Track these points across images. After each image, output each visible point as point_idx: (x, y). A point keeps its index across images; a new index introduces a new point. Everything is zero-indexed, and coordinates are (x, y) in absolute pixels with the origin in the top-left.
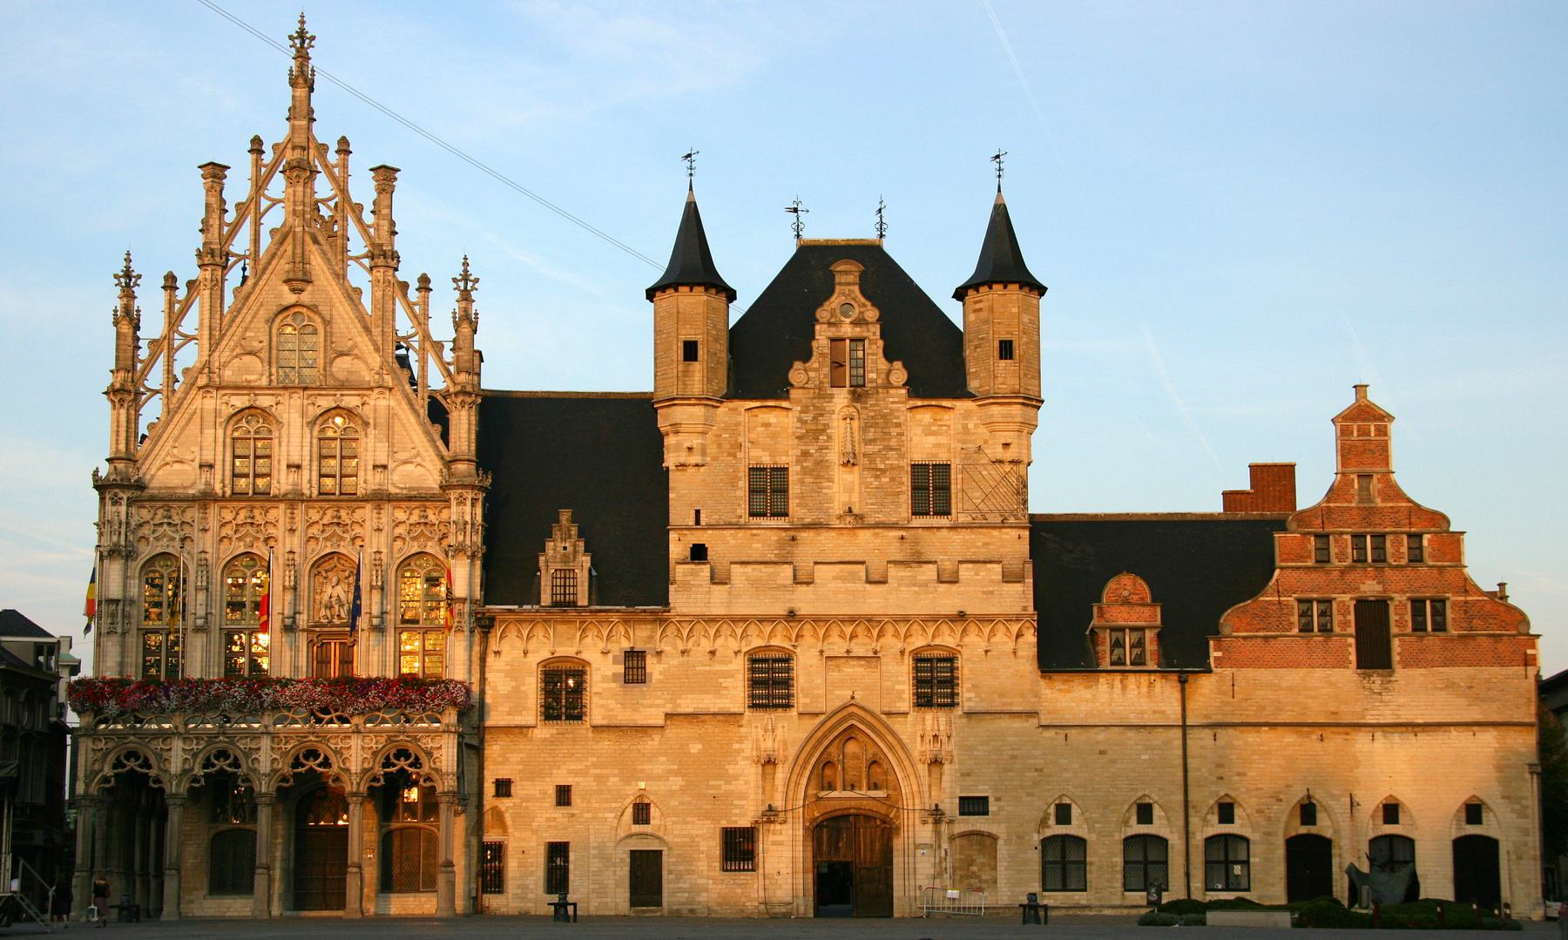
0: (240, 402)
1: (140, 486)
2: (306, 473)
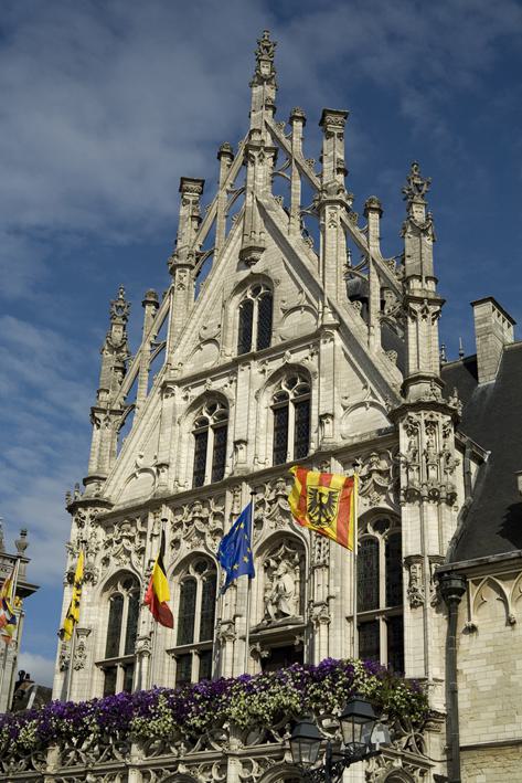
0: (197, 392)
1: (107, 504)
2: (251, 447)
